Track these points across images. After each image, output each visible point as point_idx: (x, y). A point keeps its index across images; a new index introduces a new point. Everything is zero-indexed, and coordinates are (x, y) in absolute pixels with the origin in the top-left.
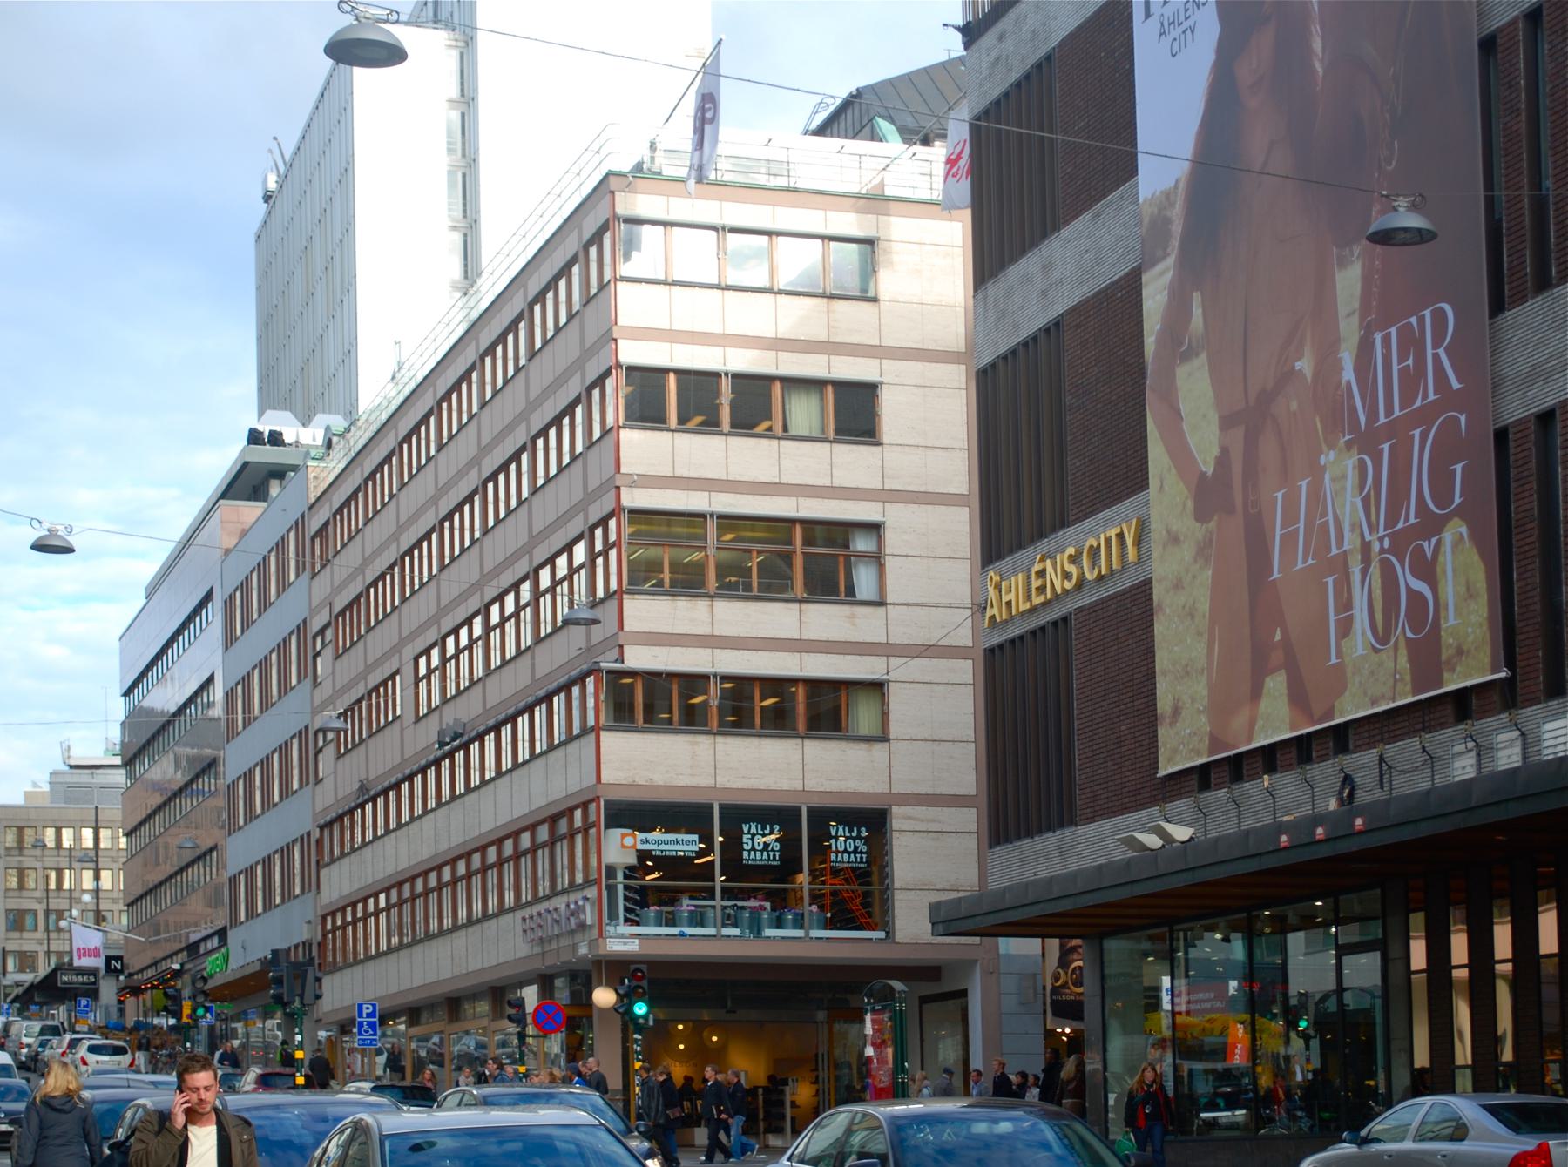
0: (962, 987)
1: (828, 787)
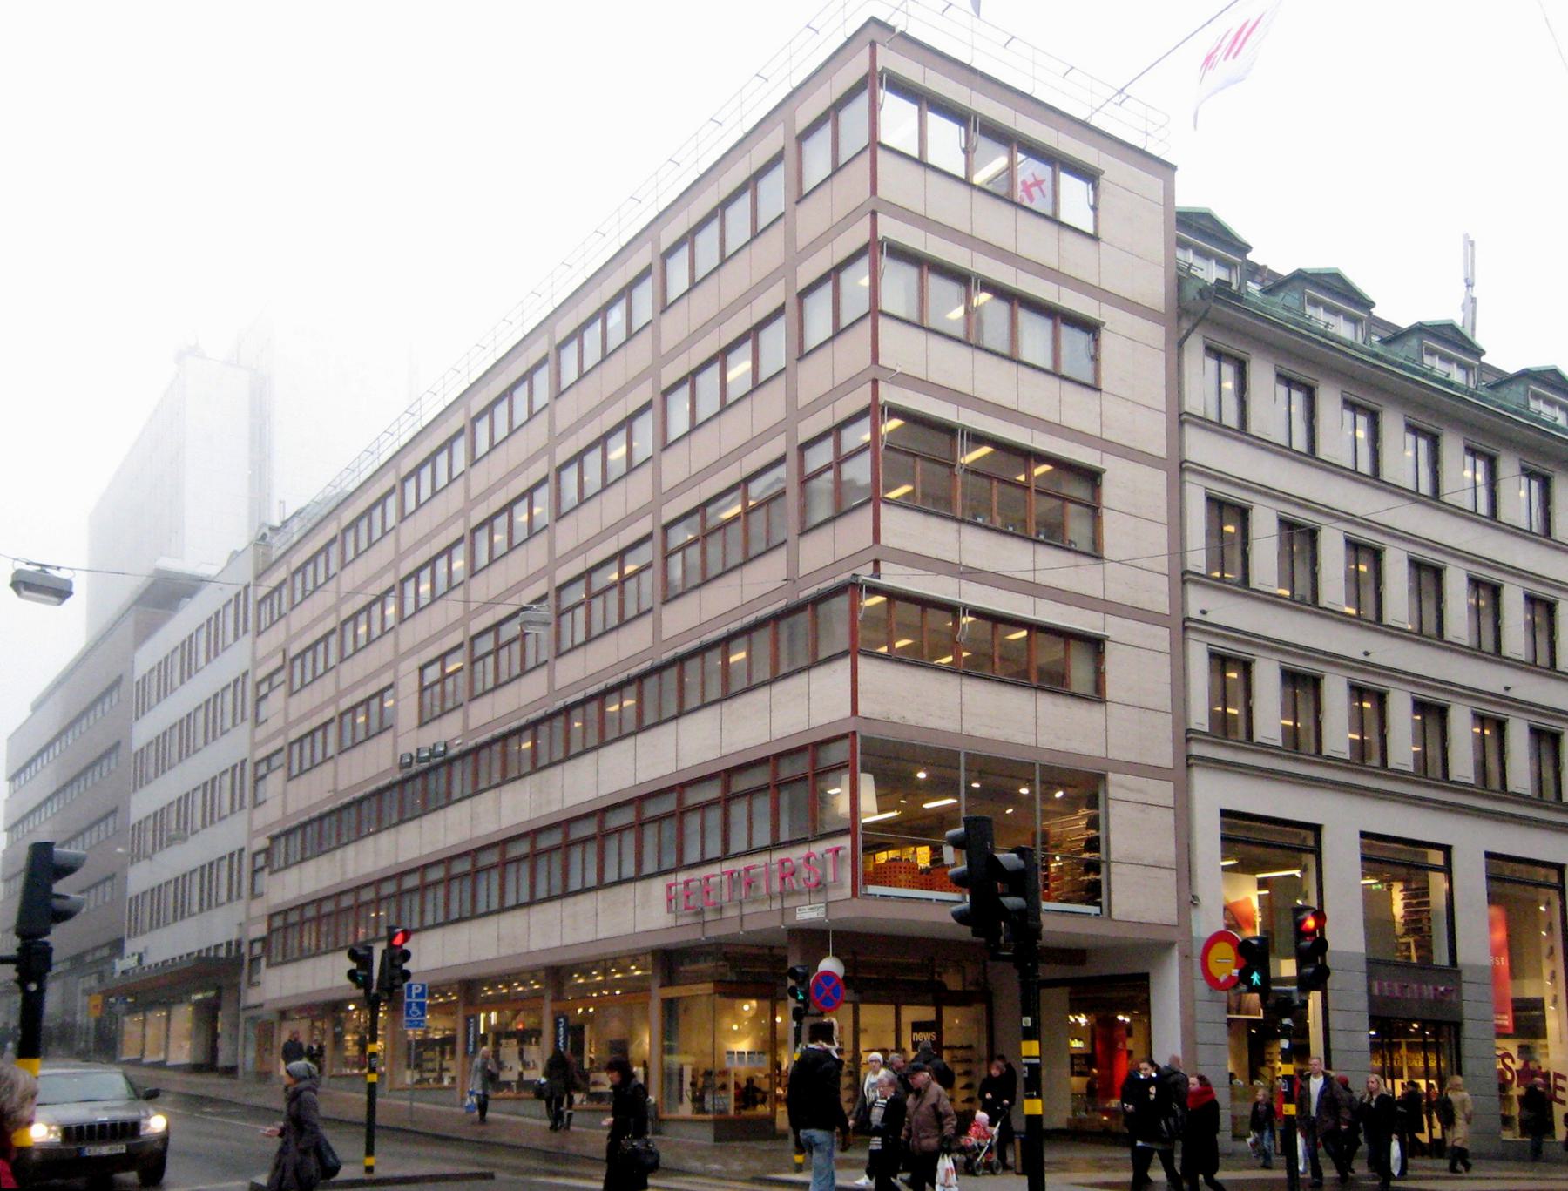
0: (1139, 969)
1: (1061, 745)
